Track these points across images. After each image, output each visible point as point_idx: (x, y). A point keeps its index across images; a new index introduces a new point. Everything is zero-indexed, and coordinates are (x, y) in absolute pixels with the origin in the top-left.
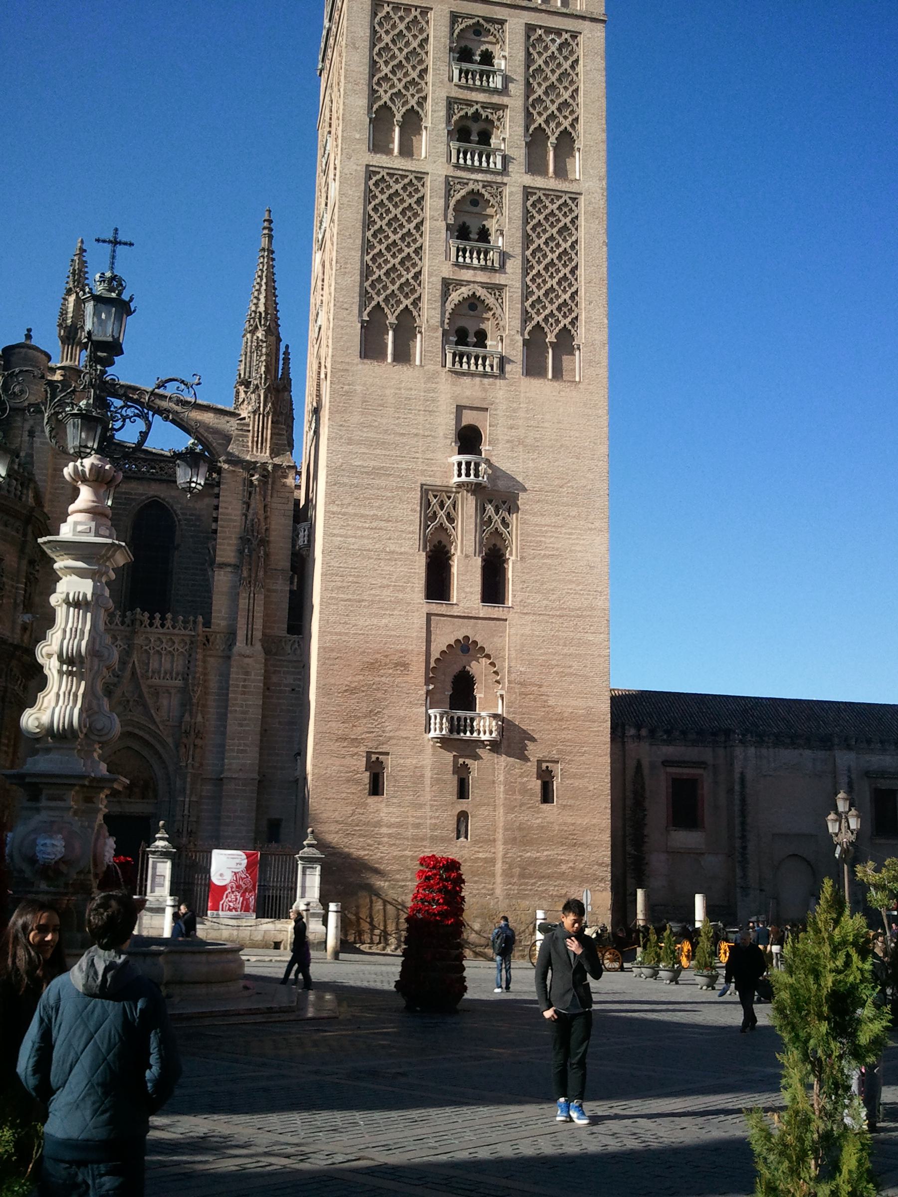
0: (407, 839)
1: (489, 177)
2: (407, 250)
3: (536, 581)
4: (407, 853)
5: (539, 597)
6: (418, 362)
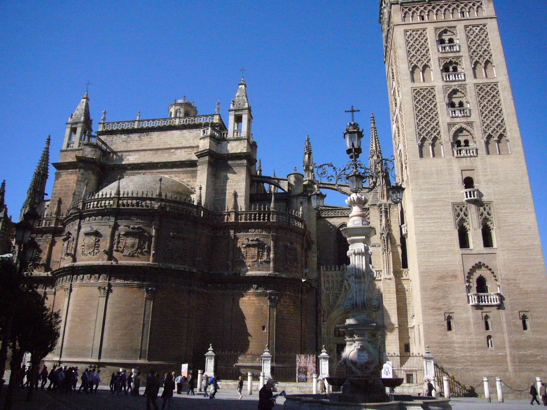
0: (466, 348)
2: (432, 115)
4: (468, 354)
5: (509, 243)
6: (443, 156)
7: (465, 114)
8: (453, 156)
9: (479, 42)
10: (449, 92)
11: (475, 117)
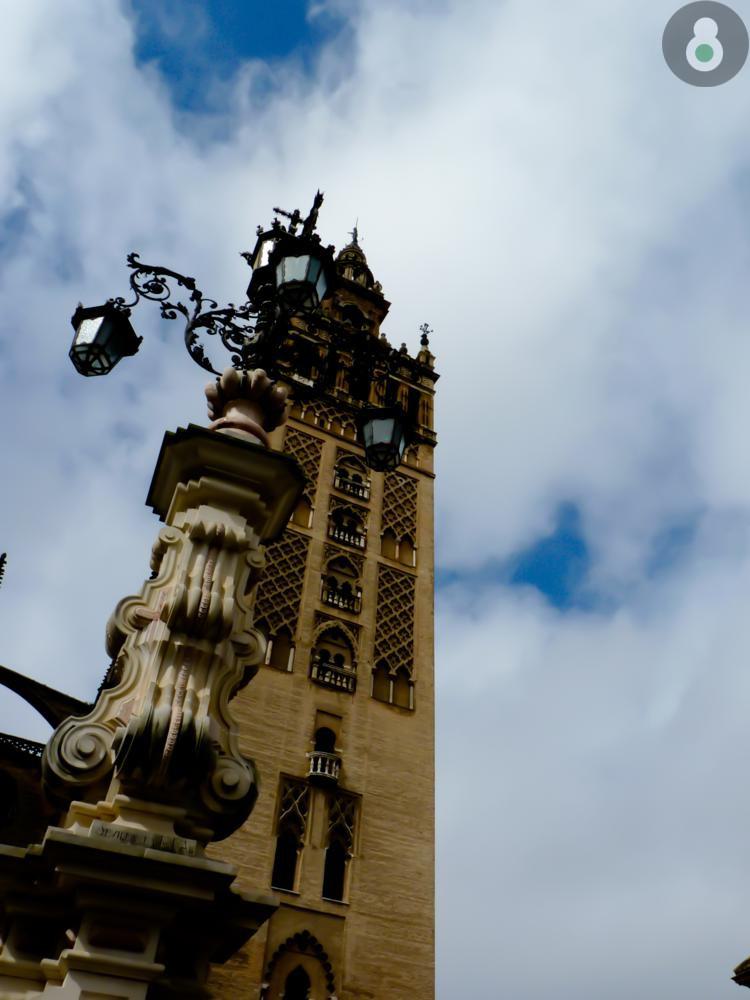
1: (354, 551)
2: (291, 585)
3: (373, 881)
5: (374, 898)
7: (351, 608)
8: (310, 676)
9: (401, 502)
10: (332, 558)
11: (367, 619)
